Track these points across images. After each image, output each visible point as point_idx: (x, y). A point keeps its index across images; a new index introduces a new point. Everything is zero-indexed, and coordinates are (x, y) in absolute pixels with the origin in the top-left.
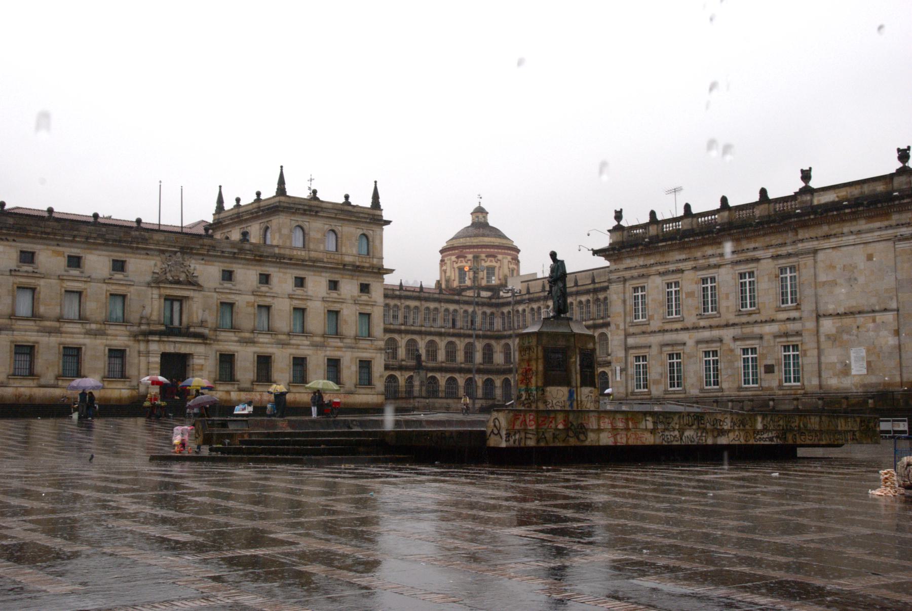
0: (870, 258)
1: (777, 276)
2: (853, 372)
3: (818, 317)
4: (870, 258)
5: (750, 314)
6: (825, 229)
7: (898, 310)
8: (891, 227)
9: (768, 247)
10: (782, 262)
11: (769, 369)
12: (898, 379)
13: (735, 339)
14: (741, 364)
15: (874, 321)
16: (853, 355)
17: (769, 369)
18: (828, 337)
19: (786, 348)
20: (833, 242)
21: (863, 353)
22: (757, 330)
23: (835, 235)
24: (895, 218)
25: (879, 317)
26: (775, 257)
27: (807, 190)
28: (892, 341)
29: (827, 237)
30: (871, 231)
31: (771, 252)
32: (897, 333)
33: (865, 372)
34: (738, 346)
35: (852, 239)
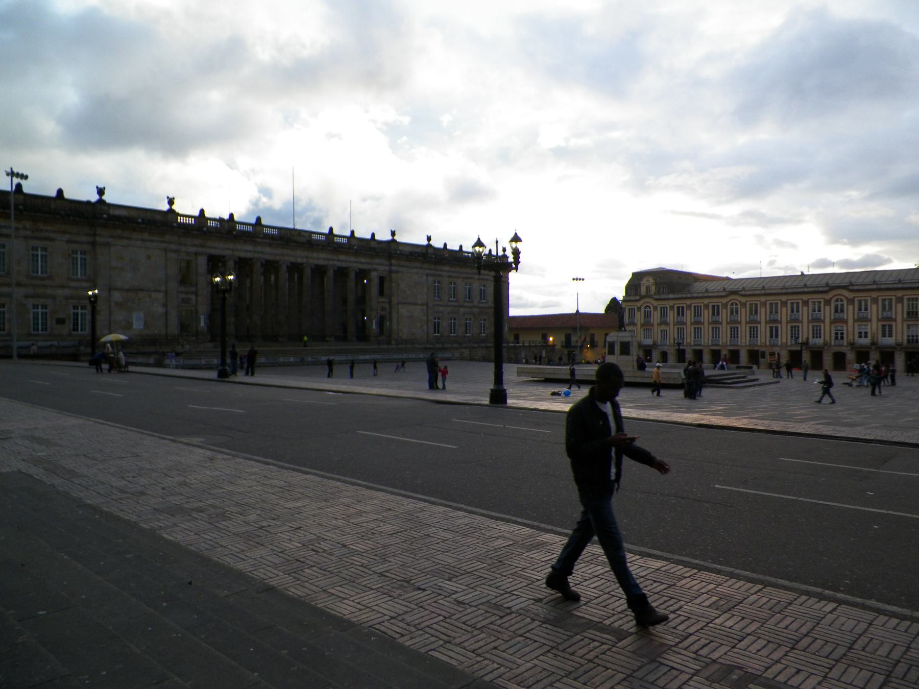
0: (149, 257)
1: (69, 255)
2: (134, 327)
3: (110, 290)
4: (149, 257)
5: (43, 279)
6: (119, 232)
7: (166, 292)
8: (165, 242)
9: (65, 232)
10: (75, 246)
11: (60, 321)
12: (164, 333)
13: (26, 297)
14: (31, 316)
15: (150, 296)
16: (134, 318)
17: (60, 321)
18: (117, 304)
19: (75, 307)
20: (125, 242)
21: (142, 315)
22: (49, 291)
23: (127, 238)
24: (167, 238)
25: (154, 295)
26: (69, 242)
27: (101, 202)
28: (161, 310)
29: (121, 238)
30: (152, 241)
31: (67, 237)
32: (165, 305)
33: (142, 327)
34: (30, 303)
35: (139, 243)
